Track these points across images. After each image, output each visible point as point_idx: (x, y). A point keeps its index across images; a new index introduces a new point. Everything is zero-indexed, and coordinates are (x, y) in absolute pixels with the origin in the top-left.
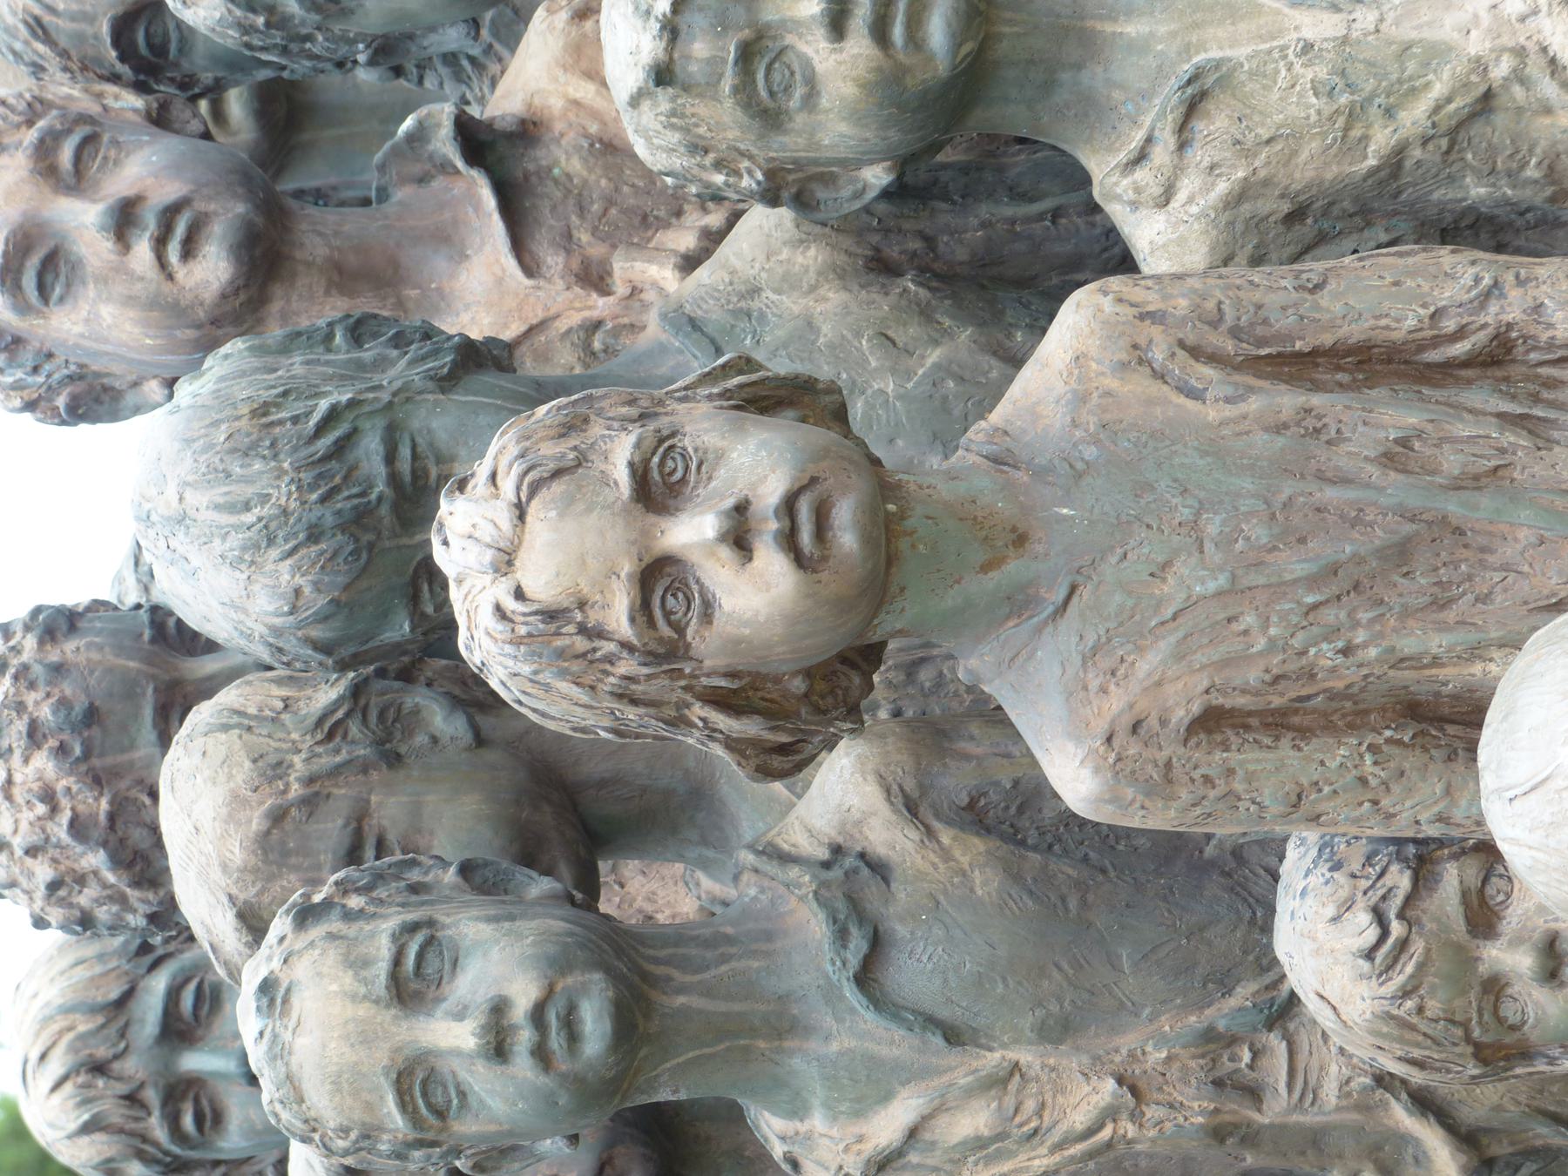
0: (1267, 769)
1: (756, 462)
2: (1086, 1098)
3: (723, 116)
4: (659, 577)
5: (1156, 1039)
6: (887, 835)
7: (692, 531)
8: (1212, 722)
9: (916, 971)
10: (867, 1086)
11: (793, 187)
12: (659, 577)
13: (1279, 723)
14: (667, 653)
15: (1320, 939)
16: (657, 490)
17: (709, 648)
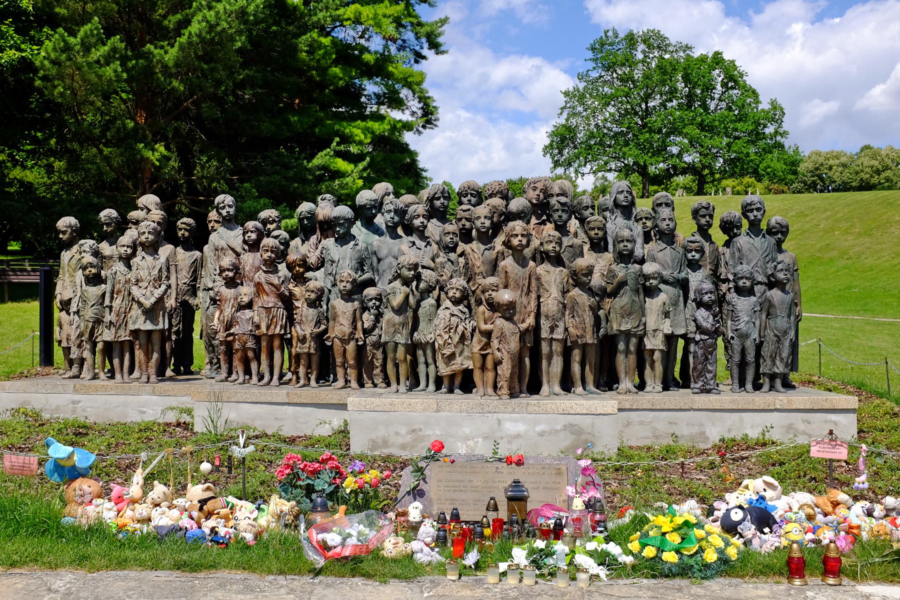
0: (503, 276)
1: (524, 242)
2: (478, 264)
3: (546, 239)
4: (517, 235)
5: (482, 269)
6: (496, 250)
7: (520, 238)
8: (506, 272)
9: (486, 252)
10: (479, 249)
11: (542, 244)
12: (517, 235)
13: (506, 277)
14: (512, 236)
15: (491, 280)
16: (522, 235)
17: (512, 239)
